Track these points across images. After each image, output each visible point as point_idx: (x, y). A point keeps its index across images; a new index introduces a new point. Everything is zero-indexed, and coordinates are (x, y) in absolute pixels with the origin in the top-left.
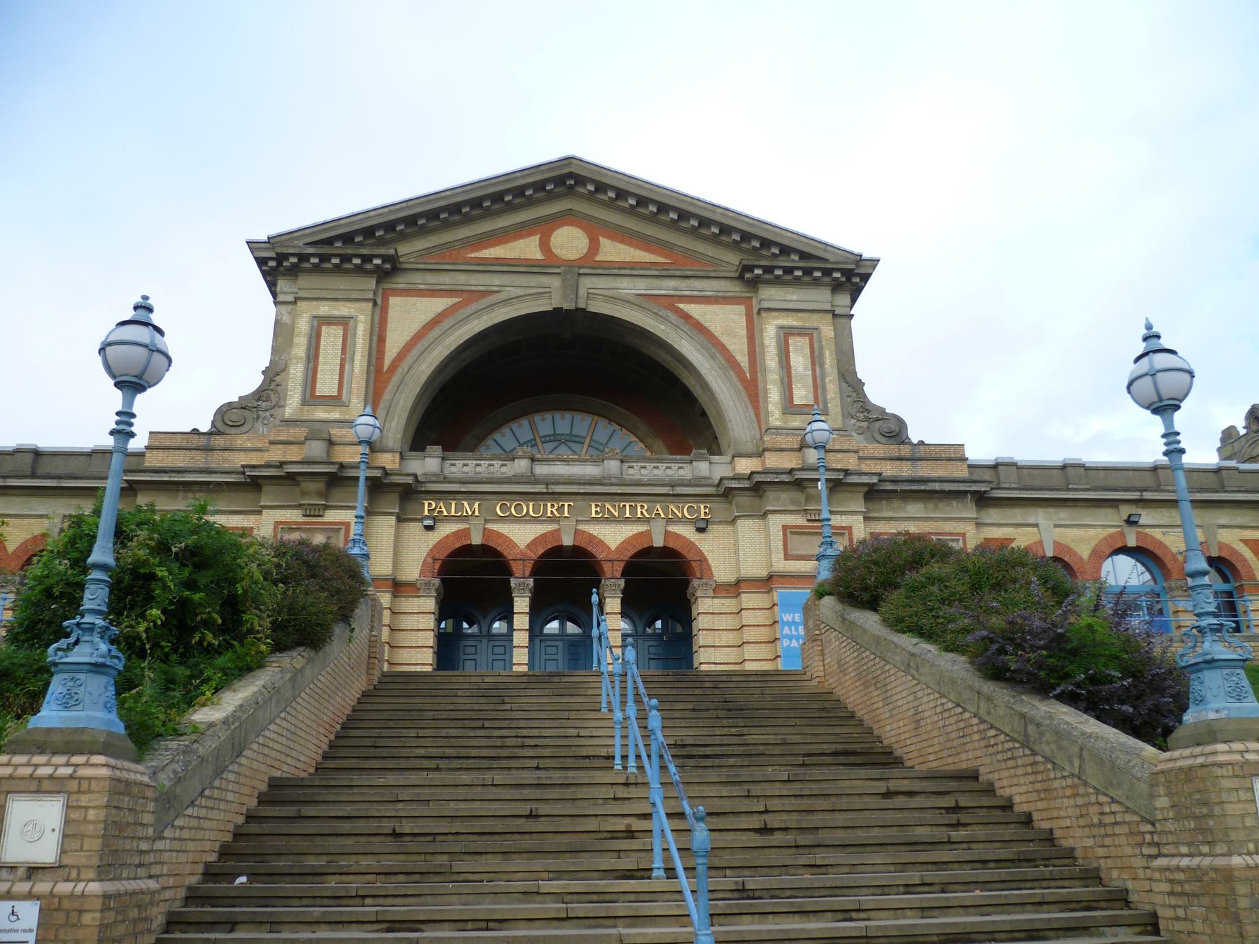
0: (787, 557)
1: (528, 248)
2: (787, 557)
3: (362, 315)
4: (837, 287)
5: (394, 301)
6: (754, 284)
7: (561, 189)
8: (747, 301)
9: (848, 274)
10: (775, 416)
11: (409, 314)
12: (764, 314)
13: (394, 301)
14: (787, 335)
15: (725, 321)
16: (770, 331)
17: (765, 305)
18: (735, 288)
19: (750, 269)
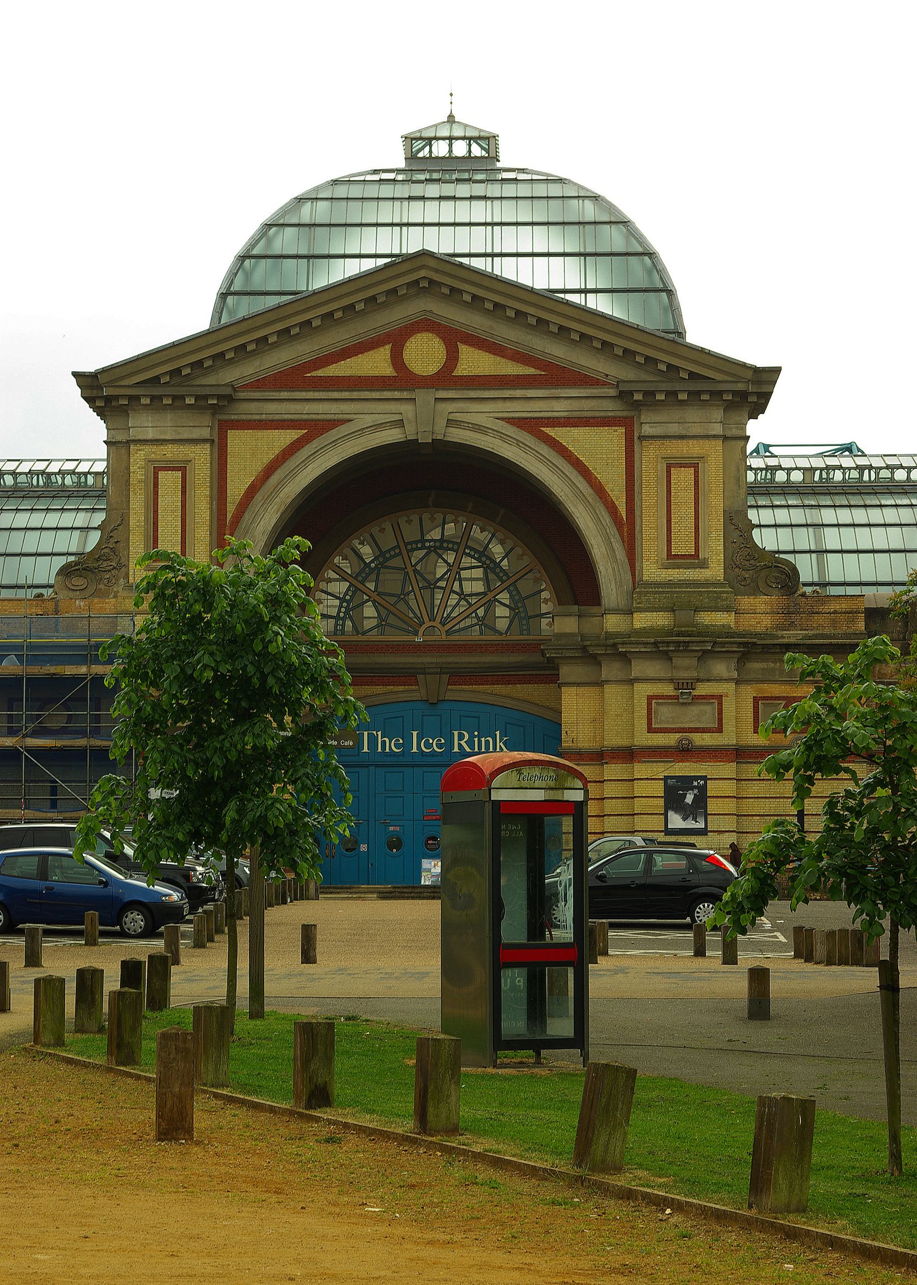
0: (650, 730)
1: (377, 363)
2: (650, 730)
3: (201, 458)
4: (729, 407)
5: (234, 437)
6: (637, 406)
7: (413, 291)
8: (627, 424)
9: (743, 396)
10: (652, 570)
11: (250, 451)
12: (645, 443)
13: (234, 437)
14: (669, 467)
15: (601, 448)
16: (650, 459)
17: (647, 430)
18: (612, 408)
19: (631, 393)
